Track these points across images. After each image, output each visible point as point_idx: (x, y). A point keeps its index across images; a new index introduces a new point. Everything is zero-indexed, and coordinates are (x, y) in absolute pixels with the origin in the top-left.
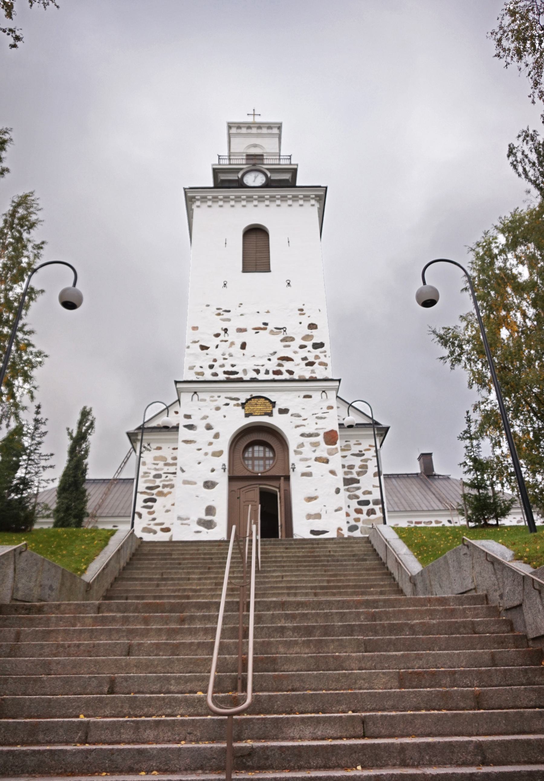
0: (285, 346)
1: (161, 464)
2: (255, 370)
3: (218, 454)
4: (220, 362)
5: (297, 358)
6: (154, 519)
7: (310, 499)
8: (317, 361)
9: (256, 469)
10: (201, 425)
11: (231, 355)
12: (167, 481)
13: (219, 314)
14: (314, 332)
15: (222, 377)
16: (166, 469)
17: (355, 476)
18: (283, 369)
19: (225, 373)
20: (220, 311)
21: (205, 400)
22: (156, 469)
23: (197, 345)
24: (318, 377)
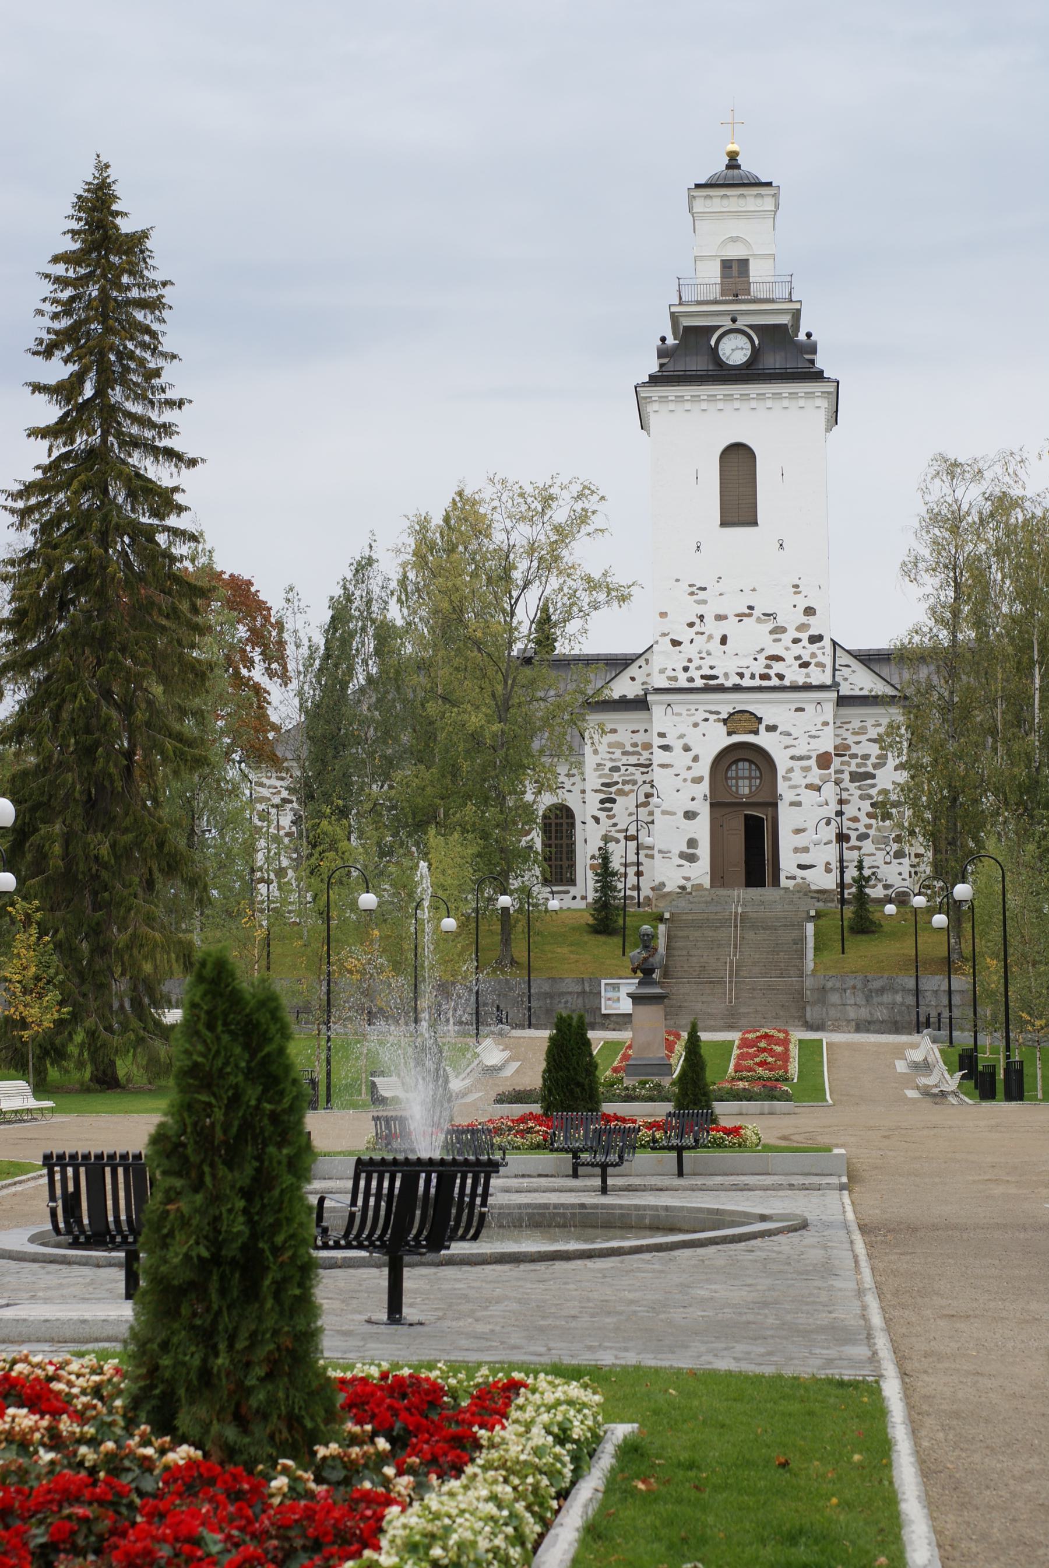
0: (775, 641)
1: (618, 753)
2: (738, 674)
3: (698, 780)
4: (697, 662)
5: (789, 657)
6: (615, 825)
7: (798, 831)
8: (813, 661)
9: (741, 791)
10: (677, 745)
11: (709, 654)
12: (628, 775)
13: (692, 594)
14: (811, 620)
15: (699, 683)
16: (624, 759)
17: (870, 769)
18: (772, 673)
19: (703, 677)
20: (694, 589)
21: (680, 714)
22: (611, 760)
23: (667, 639)
24: (814, 684)
